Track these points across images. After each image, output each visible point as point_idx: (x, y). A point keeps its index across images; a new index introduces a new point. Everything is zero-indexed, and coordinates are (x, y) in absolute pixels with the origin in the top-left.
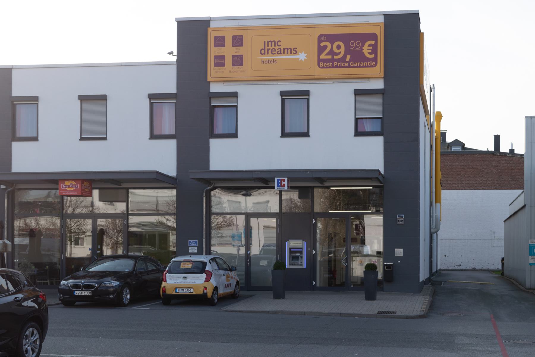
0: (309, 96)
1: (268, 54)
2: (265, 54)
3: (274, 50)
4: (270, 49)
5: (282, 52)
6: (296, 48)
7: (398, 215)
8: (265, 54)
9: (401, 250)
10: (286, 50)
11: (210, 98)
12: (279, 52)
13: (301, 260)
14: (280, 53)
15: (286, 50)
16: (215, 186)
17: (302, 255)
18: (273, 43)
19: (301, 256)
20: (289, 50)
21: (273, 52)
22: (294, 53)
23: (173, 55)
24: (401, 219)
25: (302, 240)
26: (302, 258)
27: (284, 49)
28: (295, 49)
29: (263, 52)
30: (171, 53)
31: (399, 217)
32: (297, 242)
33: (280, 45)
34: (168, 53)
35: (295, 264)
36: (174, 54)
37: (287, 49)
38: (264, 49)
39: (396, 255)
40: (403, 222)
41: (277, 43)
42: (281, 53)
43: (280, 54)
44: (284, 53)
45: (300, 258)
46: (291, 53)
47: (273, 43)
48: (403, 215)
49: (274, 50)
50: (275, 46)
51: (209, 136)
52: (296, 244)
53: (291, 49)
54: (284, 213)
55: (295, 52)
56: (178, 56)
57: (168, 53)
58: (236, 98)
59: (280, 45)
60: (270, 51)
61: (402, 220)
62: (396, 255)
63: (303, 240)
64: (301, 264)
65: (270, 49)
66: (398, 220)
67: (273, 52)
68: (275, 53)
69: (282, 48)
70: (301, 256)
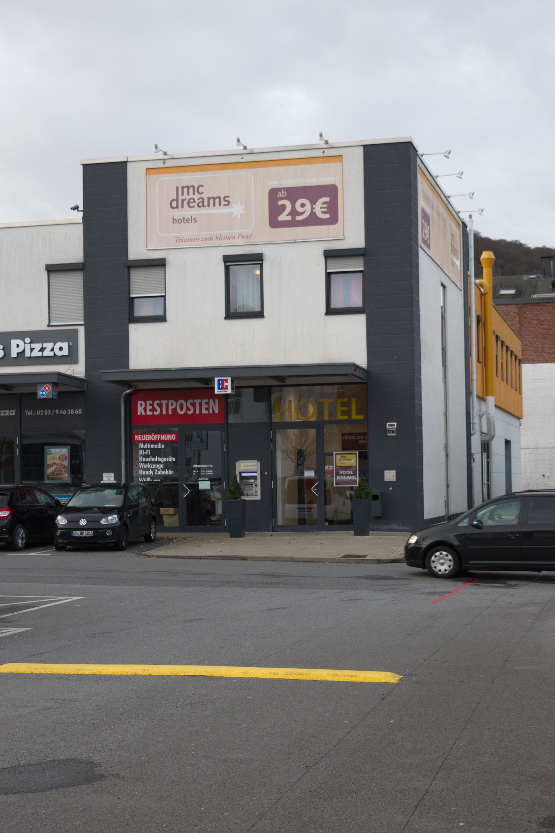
0: (262, 260)
1: (182, 207)
2: (177, 207)
3: (192, 201)
4: (186, 199)
5: (206, 203)
6: (228, 197)
7: (388, 424)
8: (177, 207)
9: (393, 472)
10: (212, 201)
11: (129, 268)
12: (201, 204)
13: (256, 489)
14: (201, 204)
15: (212, 201)
16: (137, 388)
17: (257, 482)
18: (191, 189)
19: (256, 483)
20: (217, 200)
21: (191, 205)
22: (225, 205)
23: (78, 211)
24: (392, 430)
25: (256, 461)
26: (256, 485)
27: (209, 199)
28: (227, 199)
29: (175, 204)
30: (76, 208)
31: (389, 425)
32: (249, 464)
33: (203, 193)
34: (71, 209)
35: (247, 494)
36: (79, 209)
37: (214, 199)
38: (177, 200)
39: (386, 480)
40: (395, 433)
41: (197, 189)
42: (203, 206)
43: (202, 207)
44: (209, 205)
45: (254, 485)
46: (220, 205)
47: (191, 189)
48: (395, 424)
49: (192, 201)
50: (194, 194)
51: (128, 321)
52: (248, 466)
53: (219, 198)
54: (231, 424)
55: (226, 203)
56: (85, 211)
57: (71, 209)
58: (164, 268)
59: (203, 193)
60: (185, 203)
61: (394, 430)
62: (386, 480)
63: (258, 461)
64: (256, 494)
65: (186, 199)
66: (389, 431)
67: (191, 205)
68: (194, 206)
69: (205, 196)
70: (256, 483)
